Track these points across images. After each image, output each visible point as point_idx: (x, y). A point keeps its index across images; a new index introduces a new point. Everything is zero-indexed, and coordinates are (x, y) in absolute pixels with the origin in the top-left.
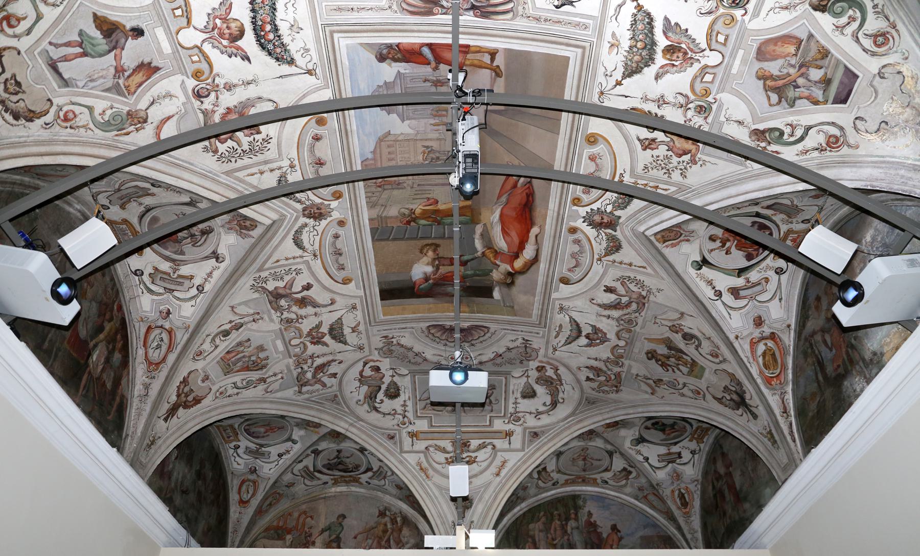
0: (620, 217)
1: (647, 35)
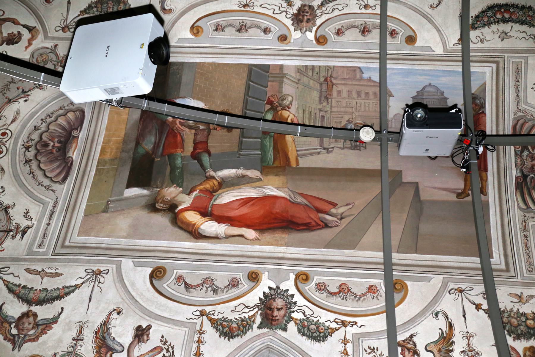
0: (285, 329)
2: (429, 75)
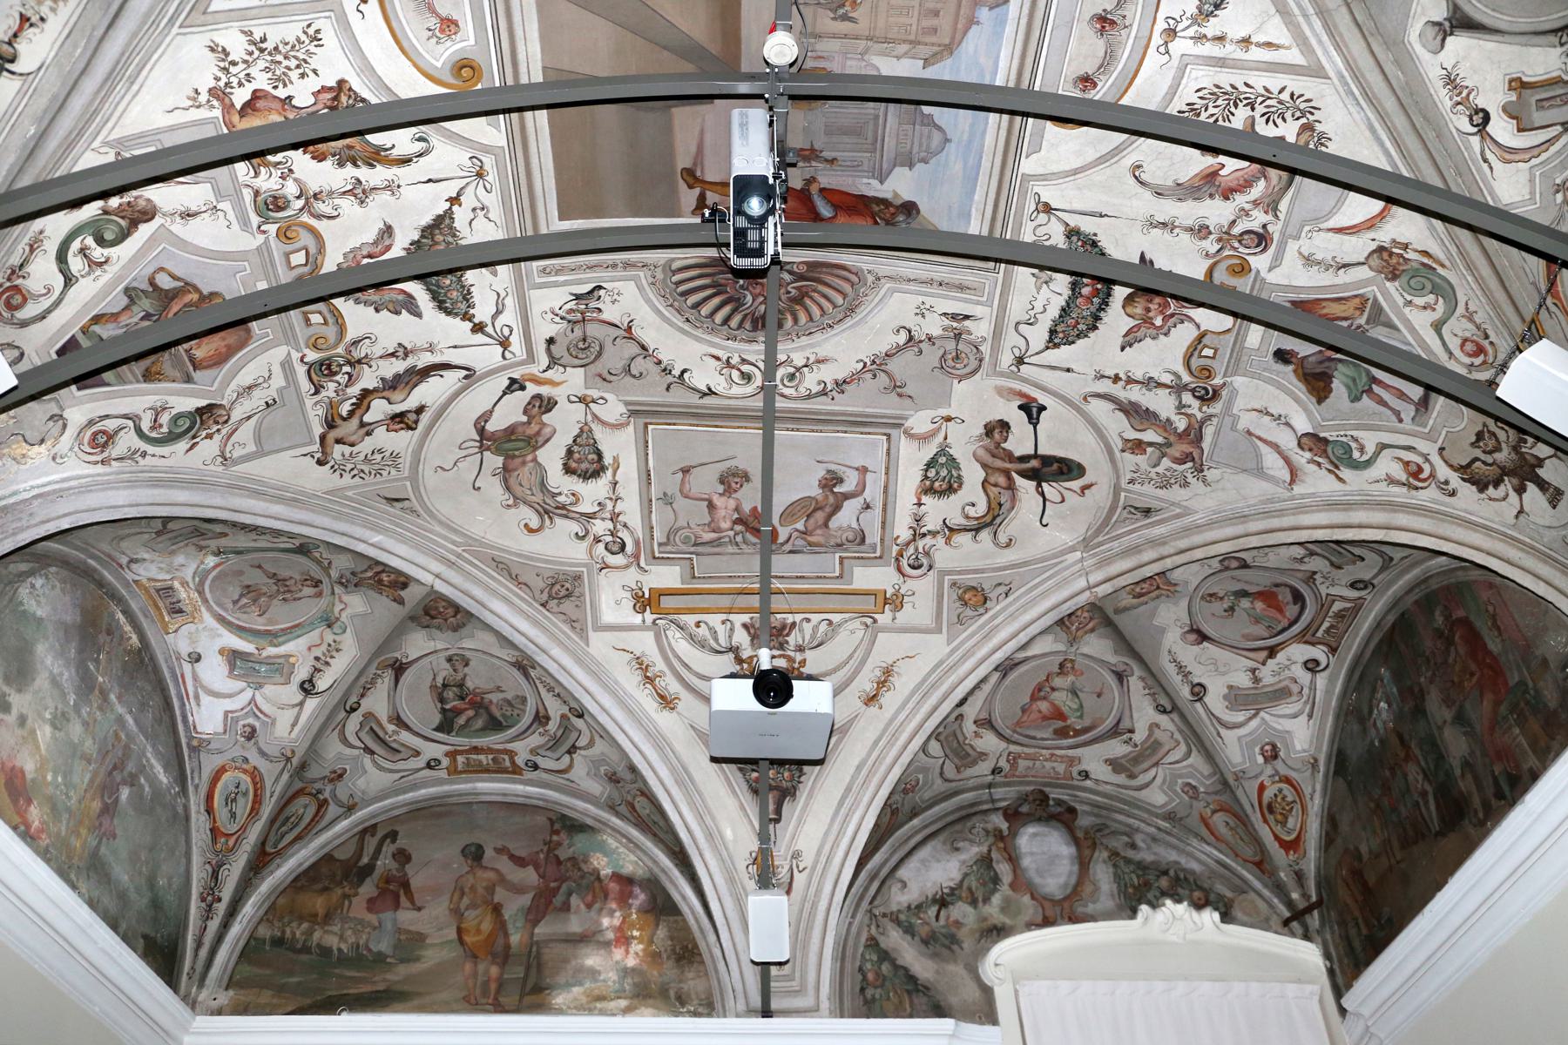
1: (438, 286)
2: (970, 141)
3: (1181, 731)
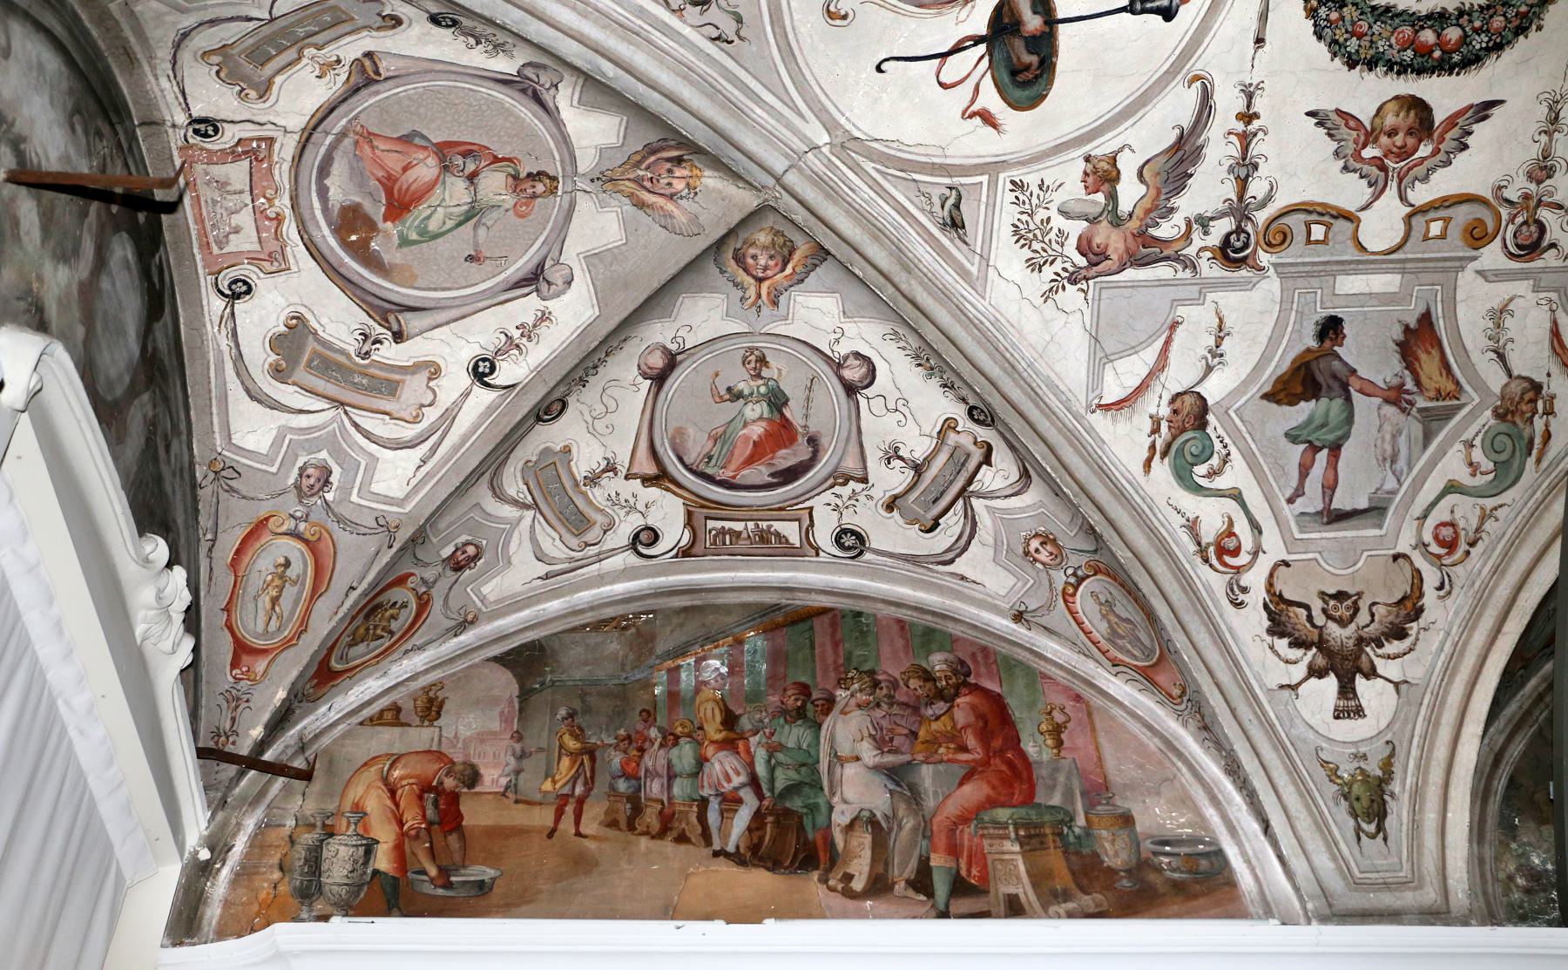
3: (450, 416)
